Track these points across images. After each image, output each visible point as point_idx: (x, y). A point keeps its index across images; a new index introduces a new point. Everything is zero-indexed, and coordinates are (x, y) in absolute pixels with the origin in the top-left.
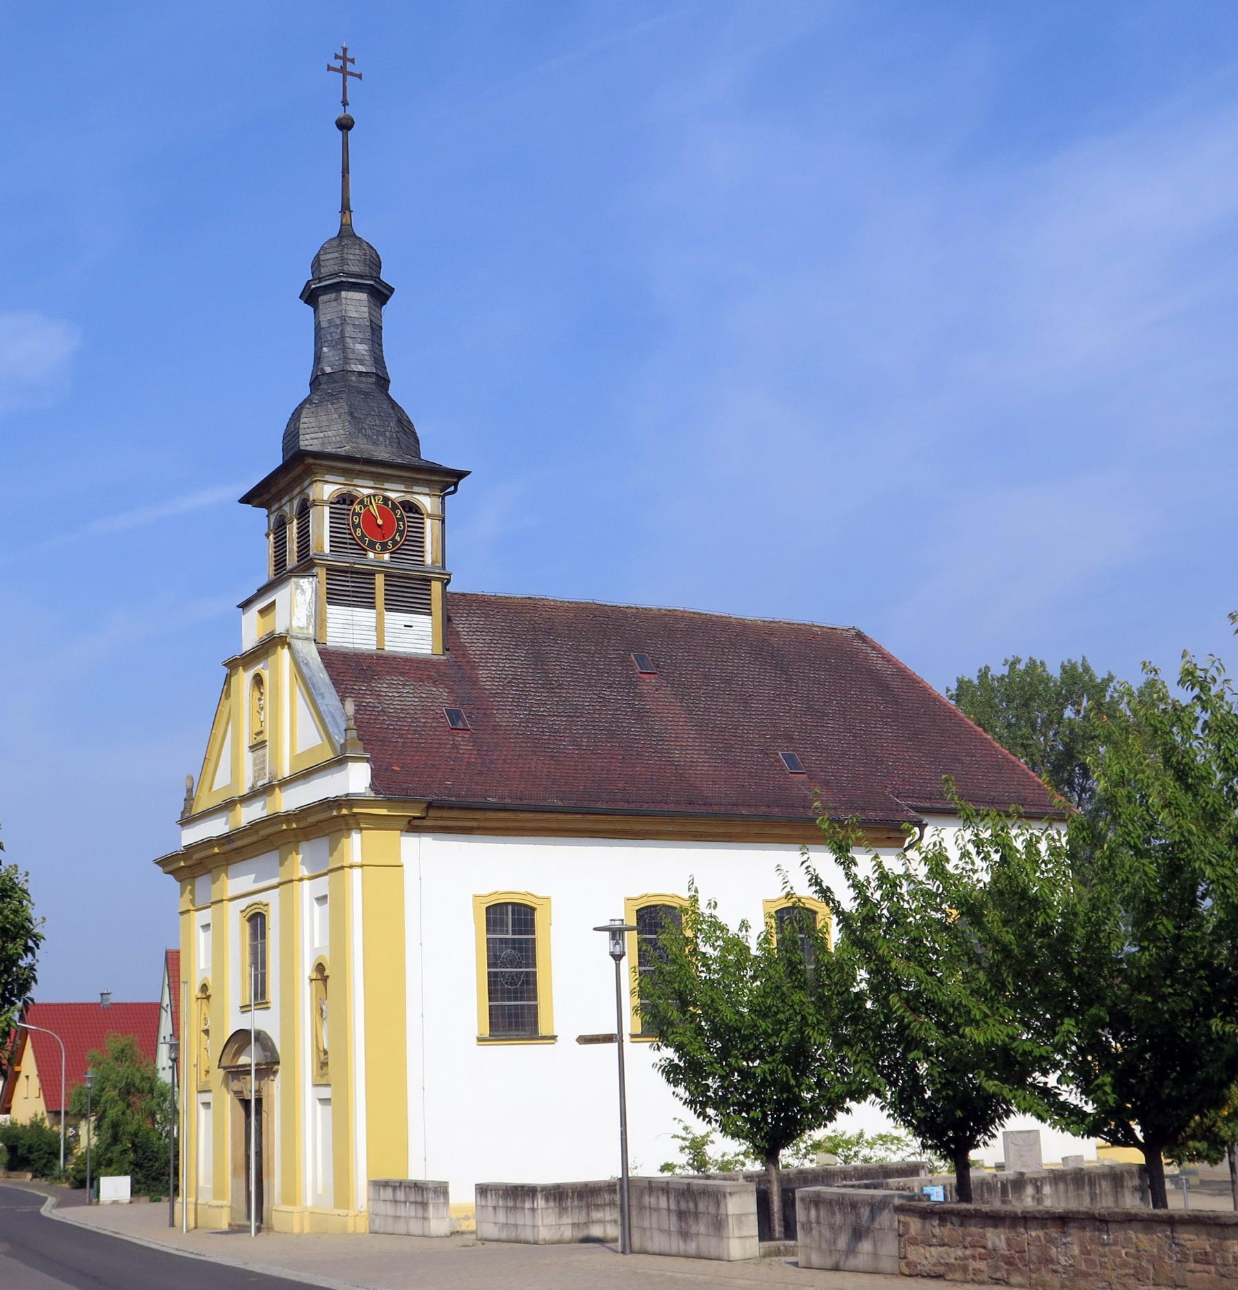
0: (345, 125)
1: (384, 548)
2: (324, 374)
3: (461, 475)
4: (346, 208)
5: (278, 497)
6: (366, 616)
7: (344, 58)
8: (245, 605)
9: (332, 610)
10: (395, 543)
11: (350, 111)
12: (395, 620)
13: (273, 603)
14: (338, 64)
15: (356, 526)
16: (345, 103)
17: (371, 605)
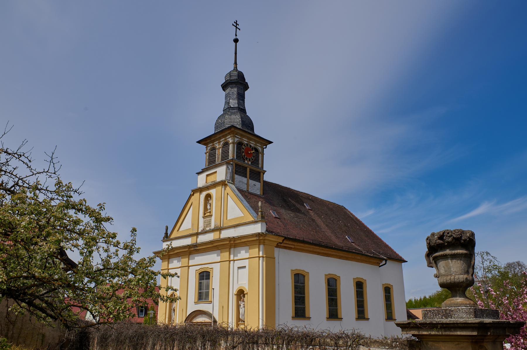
0: (236, 41)
1: (250, 160)
2: (231, 107)
3: (270, 142)
4: (236, 63)
5: (213, 142)
6: (245, 180)
7: (236, 23)
8: (199, 173)
9: (236, 176)
10: (252, 159)
11: (237, 37)
12: (252, 182)
13: (216, 172)
14: (235, 24)
15: (243, 152)
16: (236, 35)
17: (246, 177)
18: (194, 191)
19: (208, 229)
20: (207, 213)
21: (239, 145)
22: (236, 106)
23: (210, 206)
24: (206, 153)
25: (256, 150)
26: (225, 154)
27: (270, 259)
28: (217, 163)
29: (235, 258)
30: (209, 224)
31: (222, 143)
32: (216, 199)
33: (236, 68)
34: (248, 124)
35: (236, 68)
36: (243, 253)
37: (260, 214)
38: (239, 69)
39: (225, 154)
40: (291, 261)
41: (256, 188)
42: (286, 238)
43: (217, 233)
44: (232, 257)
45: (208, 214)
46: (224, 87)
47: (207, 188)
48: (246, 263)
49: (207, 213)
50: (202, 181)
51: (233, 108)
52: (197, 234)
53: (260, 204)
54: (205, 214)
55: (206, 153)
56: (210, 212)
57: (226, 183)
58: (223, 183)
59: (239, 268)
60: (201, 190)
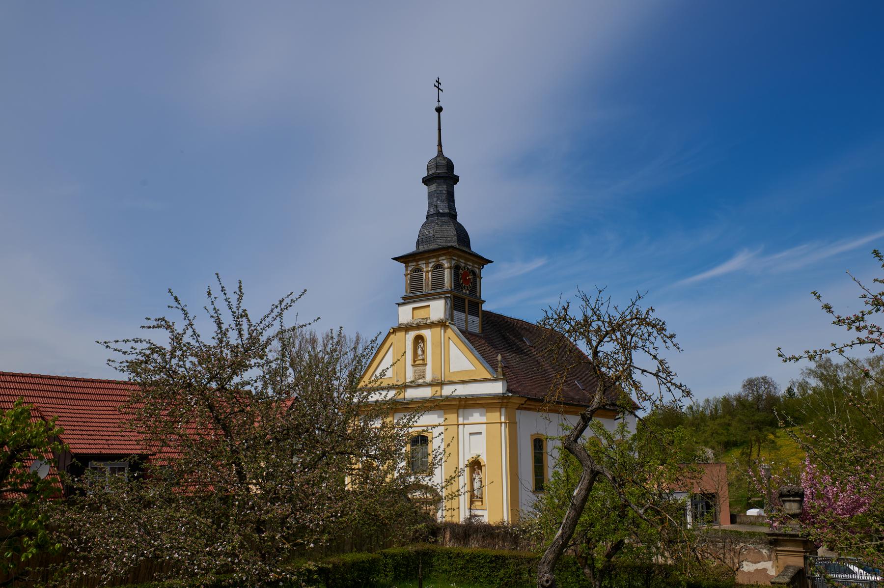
0: (439, 110)
2: (439, 213)
4: (440, 145)
6: (463, 316)
9: (455, 312)
11: (441, 104)
18: (395, 330)
19: (421, 381)
20: (419, 361)
21: (456, 269)
22: (447, 211)
23: (423, 351)
24: (406, 275)
25: (474, 273)
26: (438, 282)
27: (512, 425)
28: (425, 292)
29: (466, 422)
31: (431, 265)
32: (433, 344)
33: (440, 152)
34: (463, 236)
35: (440, 152)
36: (477, 416)
37: (500, 370)
38: (445, 154)
39: (438, 282)
40: (533, 423)
41: (475, 324)
42: (529, 399)
43: (438, 388)
44: (461, 421)
45: (421, 362)
46: (426, 181)
47: (418, 327)
48: (482, 428)
49: (419, 361)
50: (405, 314)
51: (443, 215)
53: (499, 357)
54: (415, 361)
55: (406, 275)
56: (423, 360)
57: (447, 323)
58: (442, 324)
59: (471, 434)
60: (407, 328)
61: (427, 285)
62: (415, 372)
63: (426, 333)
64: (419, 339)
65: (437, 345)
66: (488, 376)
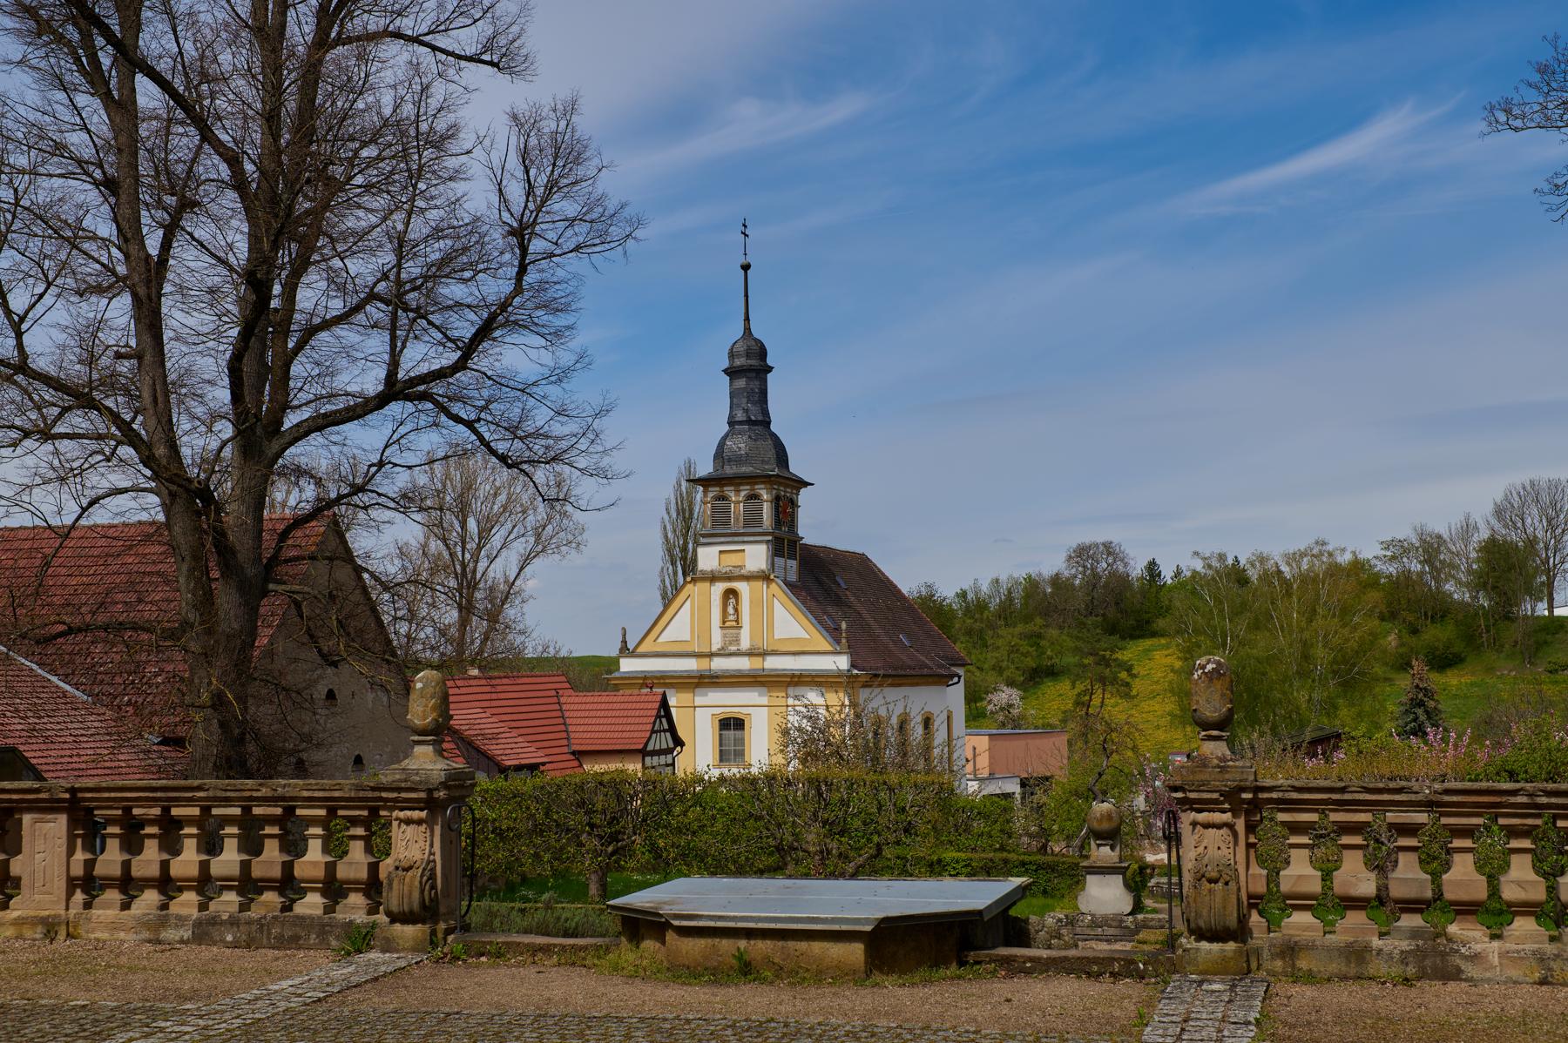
0: (746, 268)
3: (807, 484)
4: (747, 319)
11: (749, 260)
19: (733, 648)
20: (731, 622)
23: (736, 610)
26: (752, 519)
30: (737, 640)
33: (747, 330)
35: (747, 330)
38: (756, 333)
39: (752, 519)
47: (729, 578)
49: (731, 622)
52: (711, 655)
58: (764, 577)
61: (737, 519)
62: (724, 636)
63: (742, 587)
64: (731, 594)
65: (756, 603)
66: (830, 649)
